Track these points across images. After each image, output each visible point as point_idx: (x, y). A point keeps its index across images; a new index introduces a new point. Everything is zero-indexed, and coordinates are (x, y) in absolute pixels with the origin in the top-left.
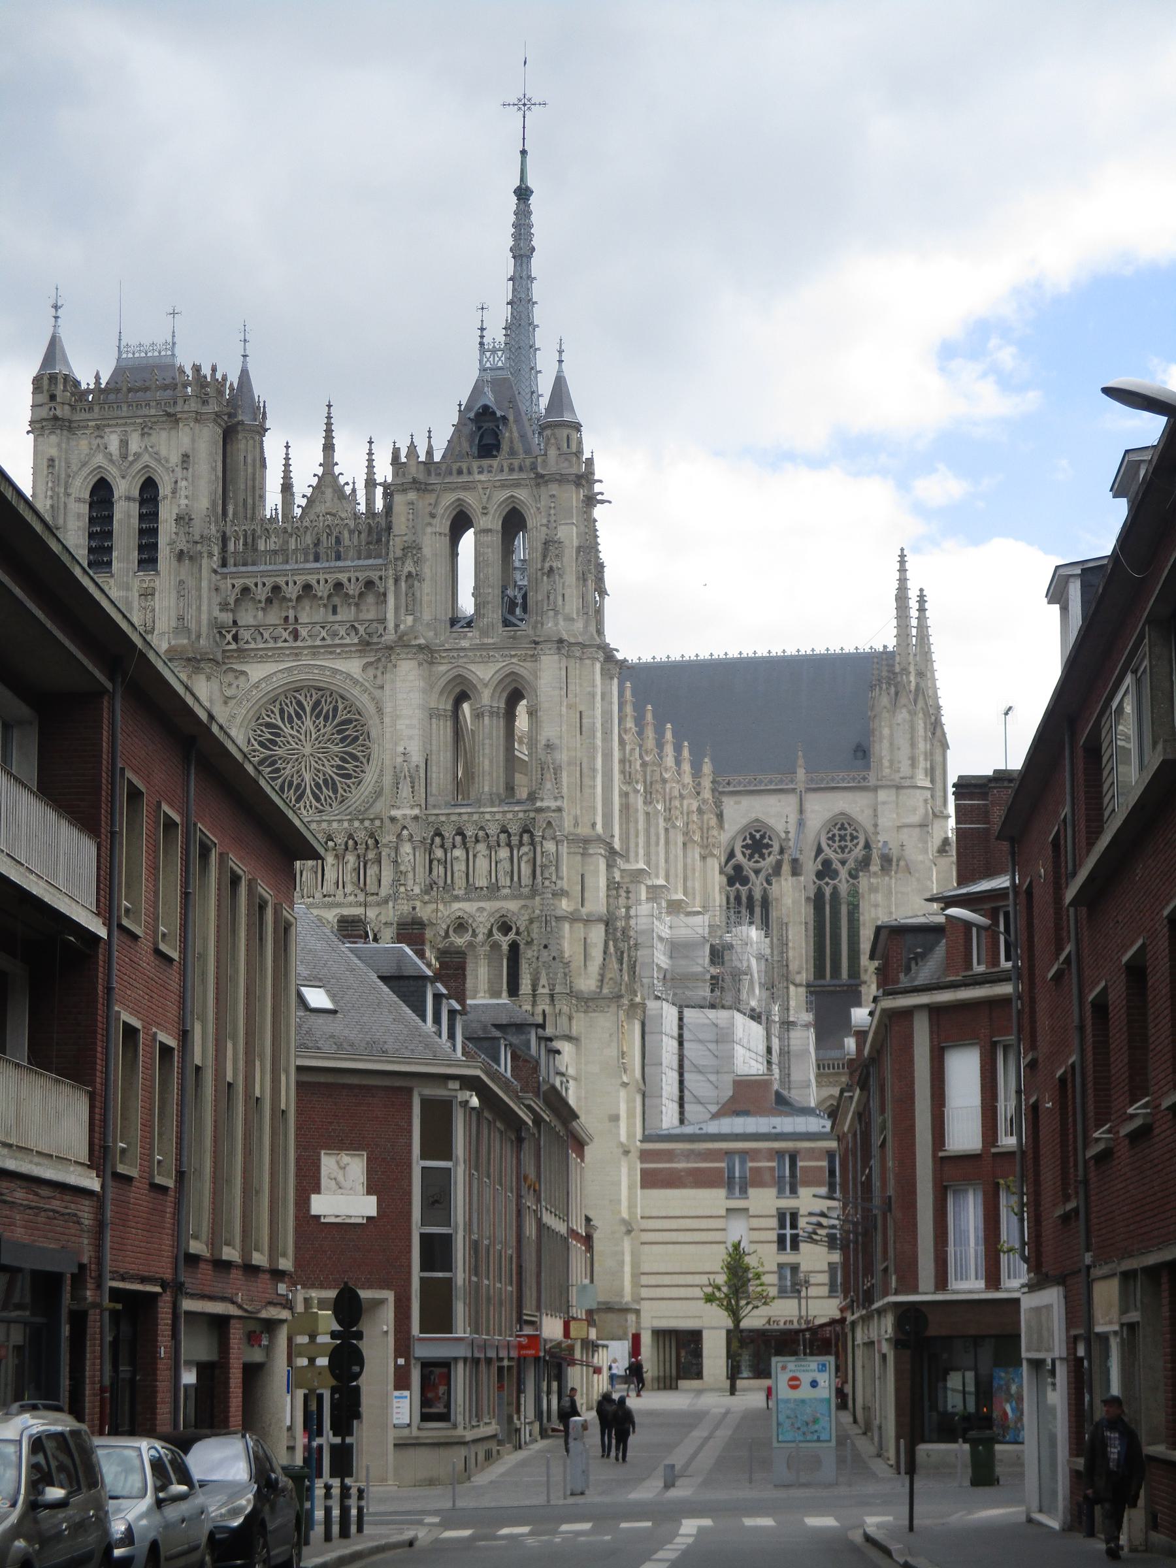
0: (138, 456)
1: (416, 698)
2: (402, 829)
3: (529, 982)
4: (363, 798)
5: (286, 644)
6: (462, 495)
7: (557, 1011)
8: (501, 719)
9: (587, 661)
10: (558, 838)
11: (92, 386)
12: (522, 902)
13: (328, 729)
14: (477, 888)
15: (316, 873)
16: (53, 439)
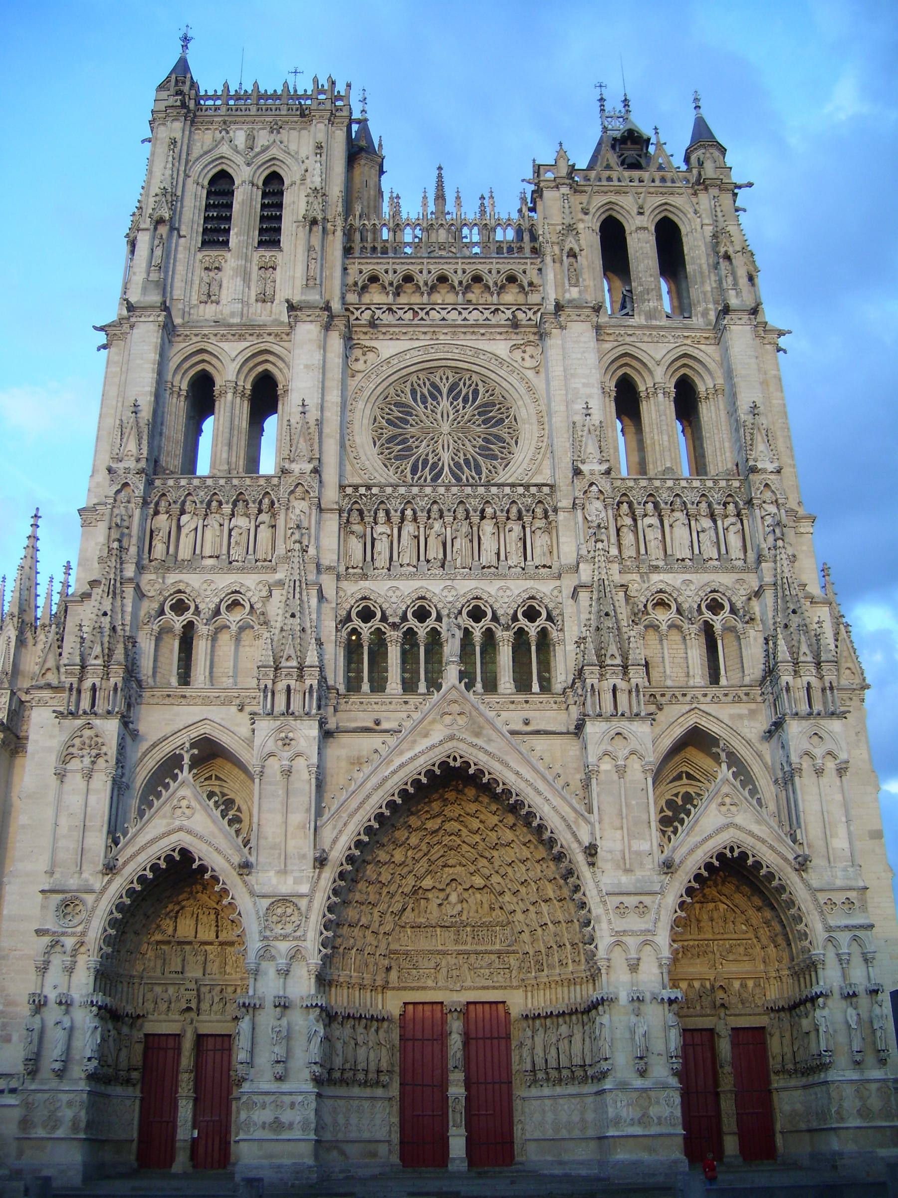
0: (265, 149)
1: (592, 358)
2: (591, 484)
3: (786, 648)
4: (516, 475)
5: (423, 322)
6: (613, 198)
7: (827, 685)
8: (672, 404)
9: (768, 347)
10: (780, 501)
11: (219, 93)
12: (735, 576)
13: (469, 410)
14: (678, 560)
15: (471, 541)
16: (178, 125)
